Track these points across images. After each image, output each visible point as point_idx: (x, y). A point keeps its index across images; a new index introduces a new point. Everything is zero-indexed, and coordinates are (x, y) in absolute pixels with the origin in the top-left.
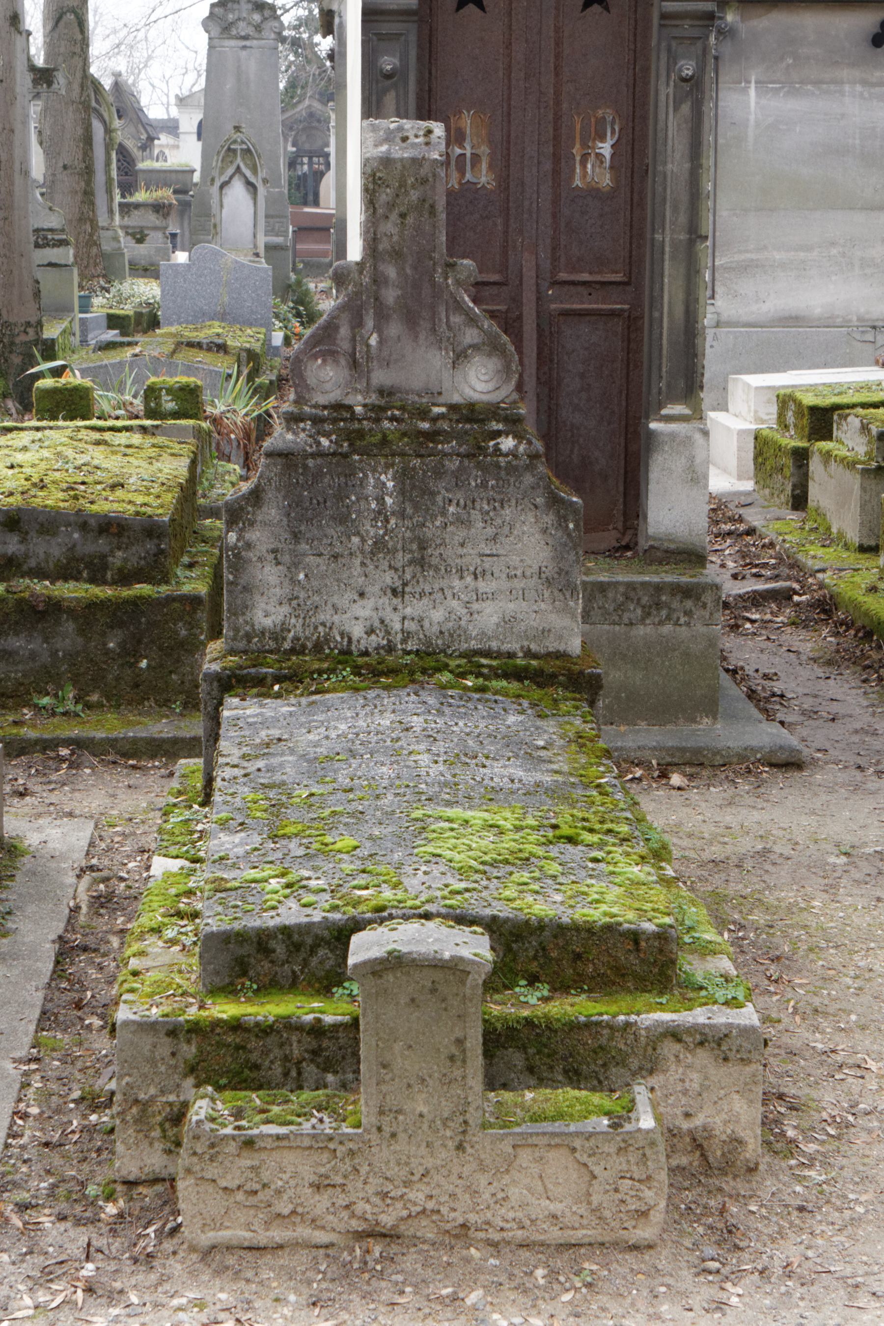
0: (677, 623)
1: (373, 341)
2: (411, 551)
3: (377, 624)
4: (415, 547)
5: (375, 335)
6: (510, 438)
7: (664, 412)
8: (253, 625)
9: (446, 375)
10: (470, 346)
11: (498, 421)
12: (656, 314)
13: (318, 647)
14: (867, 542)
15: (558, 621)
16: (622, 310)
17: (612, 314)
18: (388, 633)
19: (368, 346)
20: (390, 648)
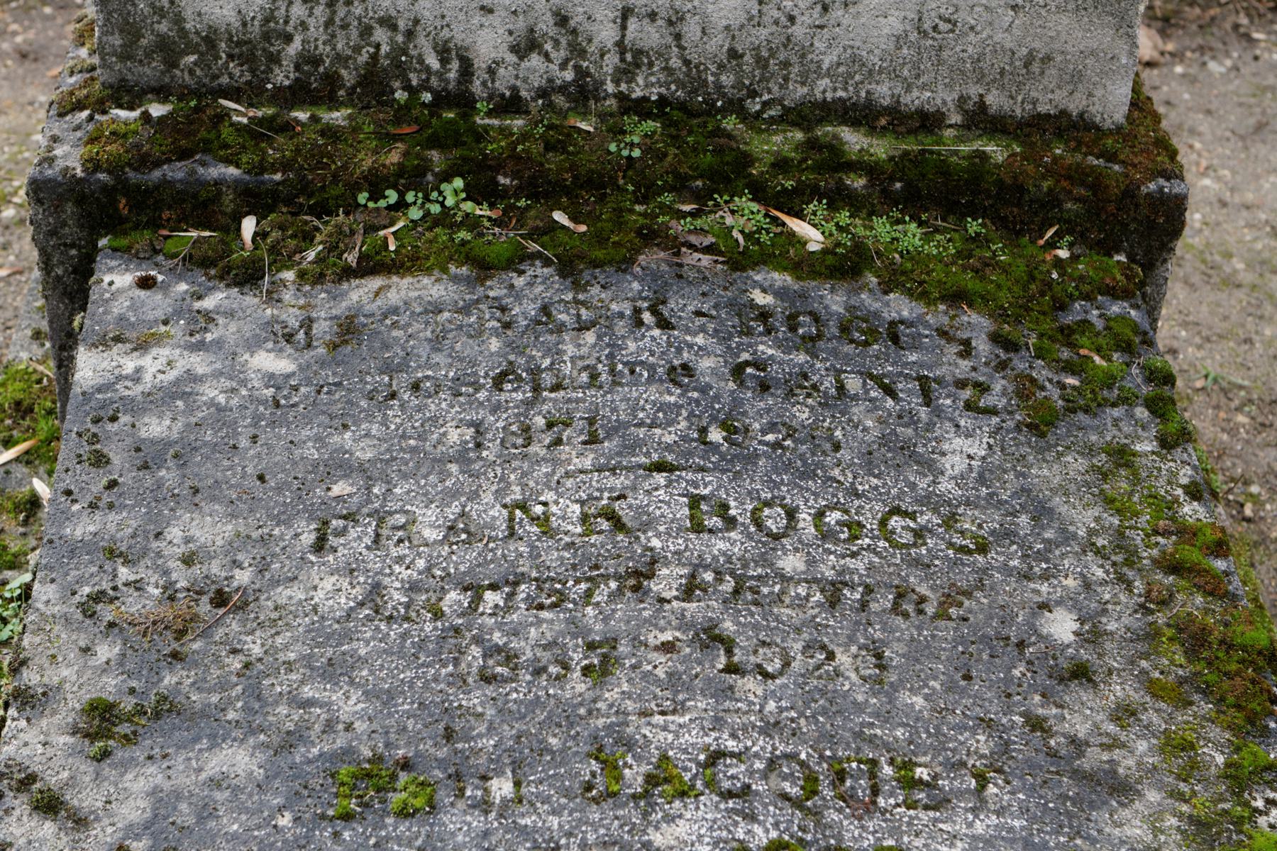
3: (546, 25)
13: (373, 85)
18: (577, 51)
20: (583, 92)
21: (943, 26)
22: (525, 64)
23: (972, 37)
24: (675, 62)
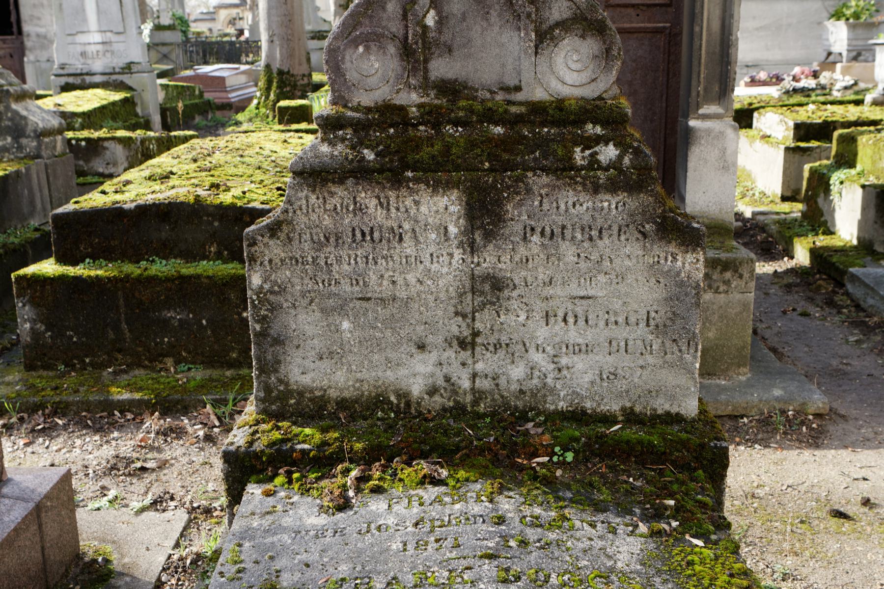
0: (717, 291)
1: (430, 20)
2: (482, 293)
3: (441, 382)
4: (487, 287)
5: (432, 12)
6: (611, 146)
7: (701, 111)
8: (287, 384)
9: (526, 64)
10: (557, 24)
11: (595, 124)
12: (697, 29)
14: (789, 194)
15: (671, 379)
16: (664, 28)
17: (656, 31)
18: (455, 392)
19: (425, 28)
21: (612, 377)
22: (433, 399)
23: (624, 381)
24: (497, 396)
